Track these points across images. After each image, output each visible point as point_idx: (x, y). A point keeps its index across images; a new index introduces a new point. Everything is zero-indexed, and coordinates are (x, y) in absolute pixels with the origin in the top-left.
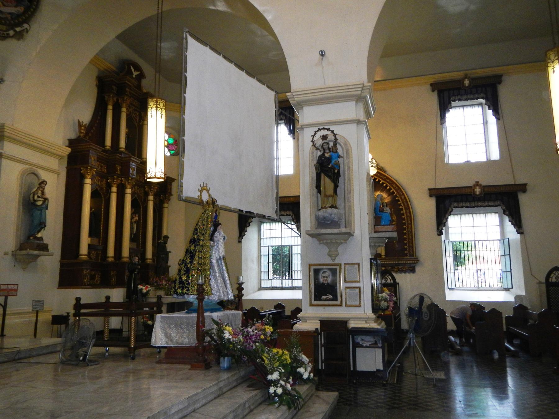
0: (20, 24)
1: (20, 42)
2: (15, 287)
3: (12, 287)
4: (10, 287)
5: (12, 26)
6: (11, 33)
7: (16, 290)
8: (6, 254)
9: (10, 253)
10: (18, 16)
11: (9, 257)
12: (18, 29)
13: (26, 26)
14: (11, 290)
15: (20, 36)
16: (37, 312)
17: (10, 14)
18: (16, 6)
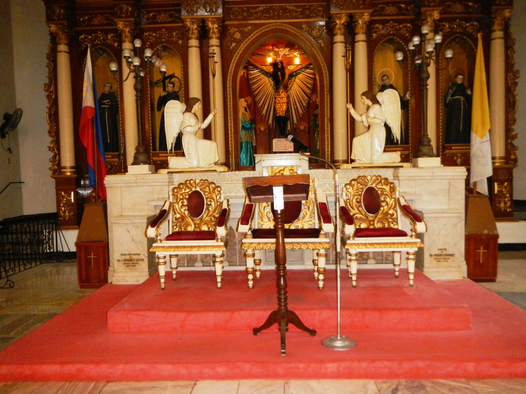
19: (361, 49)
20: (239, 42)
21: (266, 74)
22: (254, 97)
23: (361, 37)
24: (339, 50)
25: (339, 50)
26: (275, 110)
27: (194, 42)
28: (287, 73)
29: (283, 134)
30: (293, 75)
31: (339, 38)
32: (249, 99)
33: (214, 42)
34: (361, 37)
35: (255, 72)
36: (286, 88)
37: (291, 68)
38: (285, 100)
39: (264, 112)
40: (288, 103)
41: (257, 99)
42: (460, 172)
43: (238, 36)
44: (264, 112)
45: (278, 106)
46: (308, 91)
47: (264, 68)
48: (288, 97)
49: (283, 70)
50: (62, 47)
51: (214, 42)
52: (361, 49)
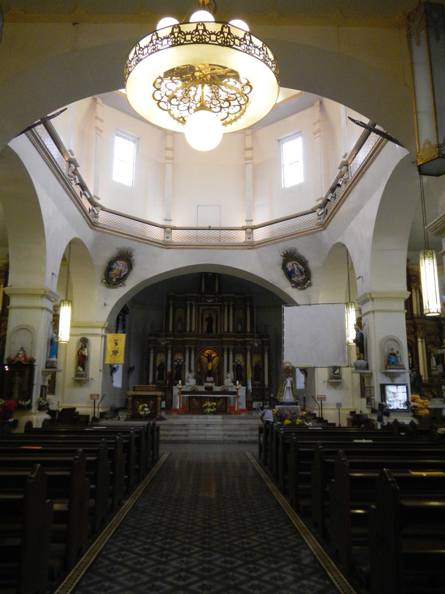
0: (306, 282)
1: (312, 287)
2: (325, 397)
3: (323, 397)
4: (322, 397)
5: (304, 284)
6: (306, 286)
7: (325, 398)
8: (324, 382)
9: (327, 381)
10: (305, 279)
11: (326, 384)
12: (307, 284)
13: (309, 281)
14: (323, 398)
15: (310, 285)
16: (339, 409)
17: (302, 279)
18: (302, 276)
19: (231, 356)
20: (199, 352)
21: (206, 357)
22: (201, 364)
23: (231, 352)
24: (225, 356)
25: (225, 356)
26: (208, 368)
27: (187, 352)
28: (212, 357)
29: (210, 376)
30: (214, 357)
31: (225, 352)
32: (200, 364)
33: (193, 352)
34: (231, 352)
35: (202, 357)
36: (212, 362)
37: (213, 355)
38: (211, 365)
39: (205, 368)
40: (212, 366)
41: (203, 364)
42: (245, 388)
43: (199, 350)
44: (205, 368)
45: (209, 367)
46: (218, 362)
47: (205, 355)
48: (212, 364)
49: (211, 355)
50: (152, 351)
51: (193, 352)
52: (231, 356)
